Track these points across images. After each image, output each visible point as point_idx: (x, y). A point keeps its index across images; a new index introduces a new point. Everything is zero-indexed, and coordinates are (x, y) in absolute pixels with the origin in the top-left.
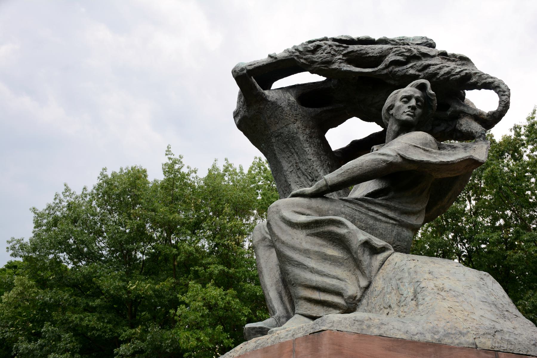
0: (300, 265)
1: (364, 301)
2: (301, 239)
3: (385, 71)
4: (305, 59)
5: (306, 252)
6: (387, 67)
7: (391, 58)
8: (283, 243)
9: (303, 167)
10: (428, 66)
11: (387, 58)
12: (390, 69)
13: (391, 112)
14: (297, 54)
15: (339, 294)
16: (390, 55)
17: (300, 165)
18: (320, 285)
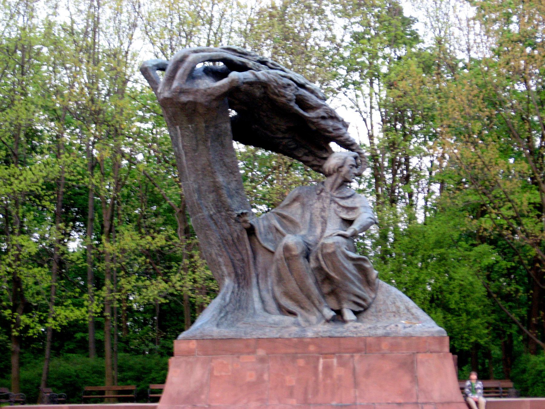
0: (353, 283)
1: (373, 305)
2: (350, 266)
3: (315, 120)
4: (279, 91)
5: (354, 275)
6: (318, 118)
7: (321, 112)
8: (345, 268)
9: (227, 160)
10: (339, 129)
11: (318, 111)
12: (319, 120)
13: (340, 169)
14: (275, 84)
15: (364, 300)
16: (321, 110)
17: (225, 157)
18: (360, 295)
